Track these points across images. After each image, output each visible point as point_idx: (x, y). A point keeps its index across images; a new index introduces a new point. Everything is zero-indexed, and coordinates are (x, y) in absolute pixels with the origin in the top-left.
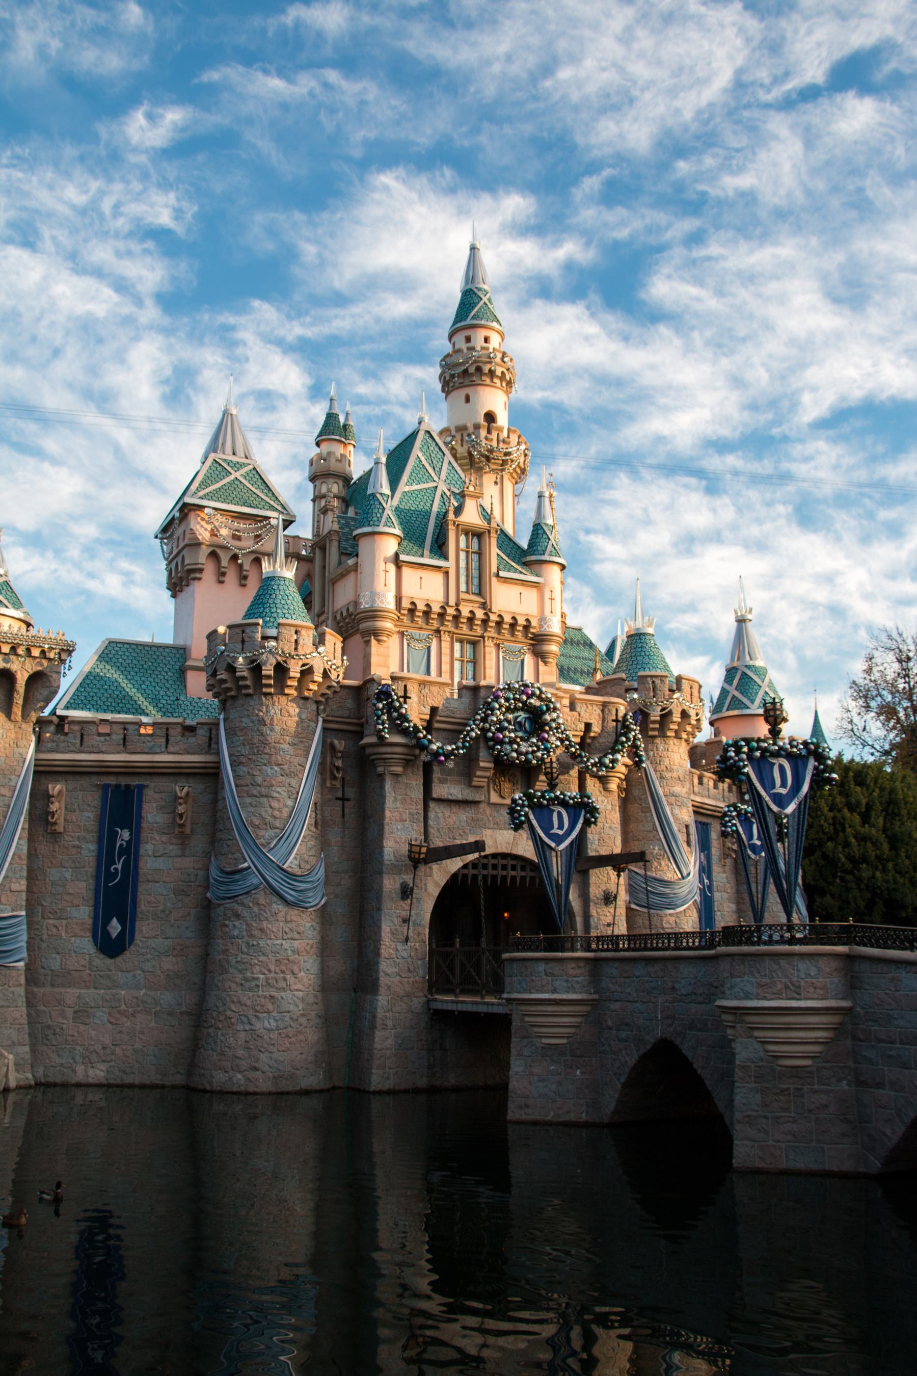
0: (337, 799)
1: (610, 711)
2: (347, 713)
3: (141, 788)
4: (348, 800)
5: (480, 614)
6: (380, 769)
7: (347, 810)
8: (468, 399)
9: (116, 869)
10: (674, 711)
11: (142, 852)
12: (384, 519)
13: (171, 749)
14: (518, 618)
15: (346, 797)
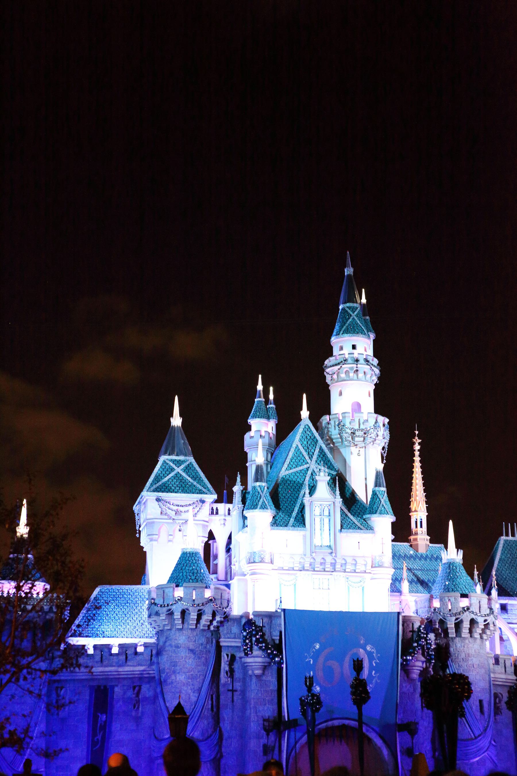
0: (229, 690)
1: (408, 625)
2: (233, 636)
3: (113, 687)
4: (236, 691)
5: (329, 559)
6: (250, 672)
7: (235, 698)
8: (341, 394)
9: (98, 739)
10: (464, 620)
11: (113, 729)
12: (260, 503)
13: (129, 663)
14: (357, 559)
15: (234, 689)
